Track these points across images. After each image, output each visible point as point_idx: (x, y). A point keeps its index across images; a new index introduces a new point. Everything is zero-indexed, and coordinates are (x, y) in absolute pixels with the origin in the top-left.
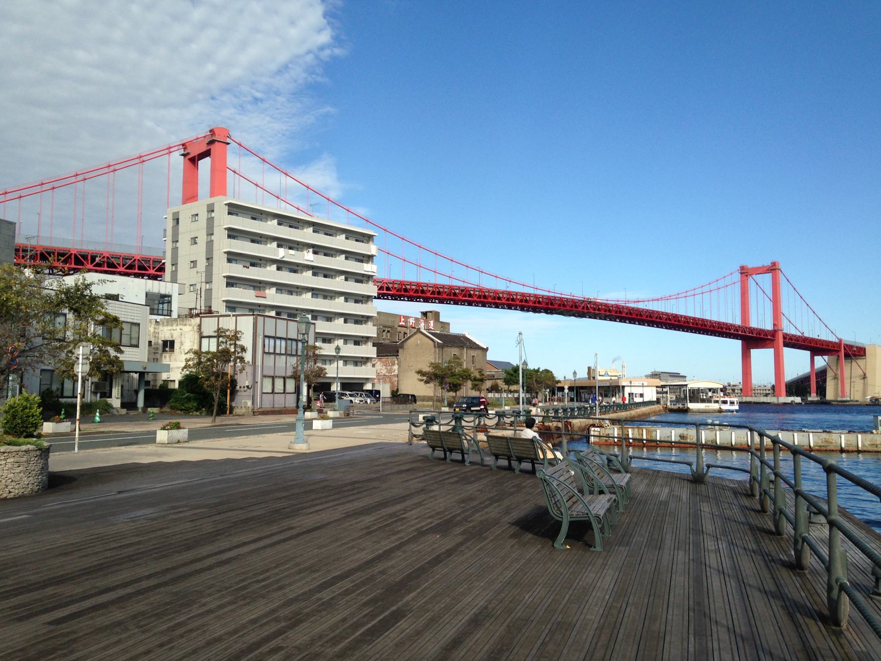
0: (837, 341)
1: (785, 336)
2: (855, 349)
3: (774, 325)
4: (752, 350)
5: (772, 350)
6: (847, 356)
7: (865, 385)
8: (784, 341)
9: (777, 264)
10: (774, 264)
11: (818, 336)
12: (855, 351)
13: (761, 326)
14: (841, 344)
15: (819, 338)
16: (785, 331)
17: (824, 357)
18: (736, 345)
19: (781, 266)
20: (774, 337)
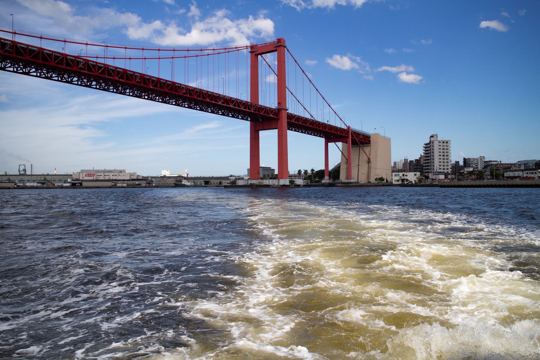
0: (346, 128)
1: (290, 117)
2: (361, 137)
3: (279, 104)
4: (260, 132)
5: (277, 130)
6: (354, 143)
7: (369, 168)
8: (288, 122)
9: (282, 41)
10: (279, 40)
11: (328, 121)
12: (361, 139)
13: (268, 105)
14: (349, 131)
15: (329, 123)
16: (290, 111)
17: (338, 143)
18: (245, 125)
19: (287, 44)
20: (278, 116)
